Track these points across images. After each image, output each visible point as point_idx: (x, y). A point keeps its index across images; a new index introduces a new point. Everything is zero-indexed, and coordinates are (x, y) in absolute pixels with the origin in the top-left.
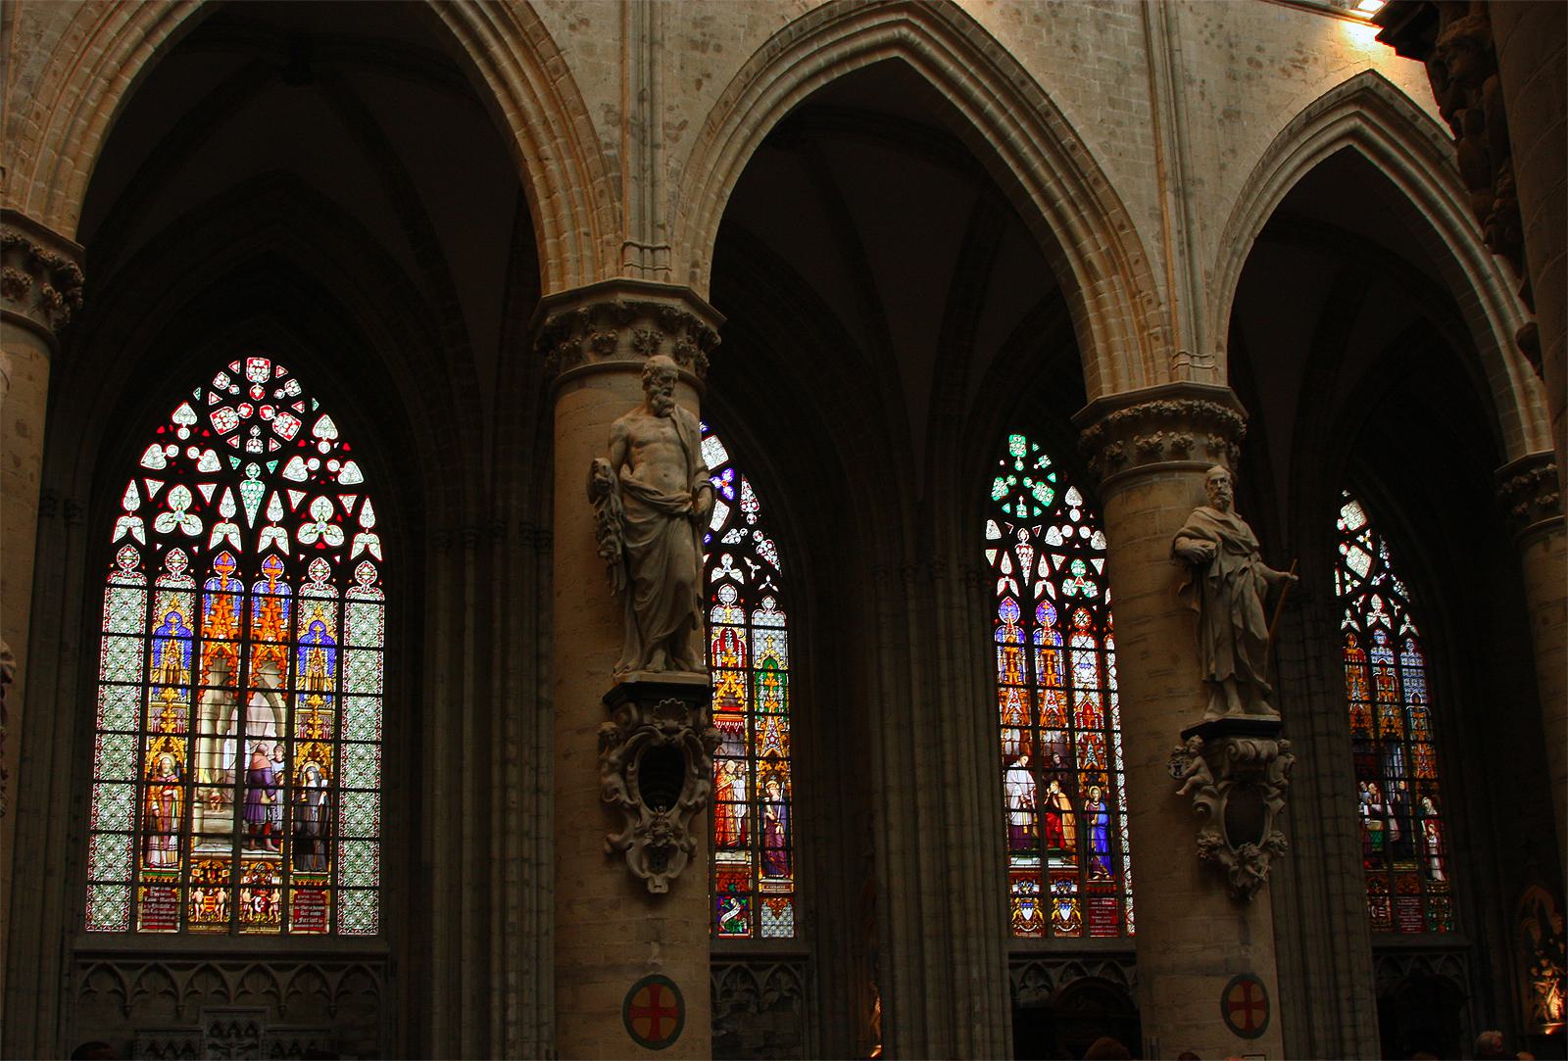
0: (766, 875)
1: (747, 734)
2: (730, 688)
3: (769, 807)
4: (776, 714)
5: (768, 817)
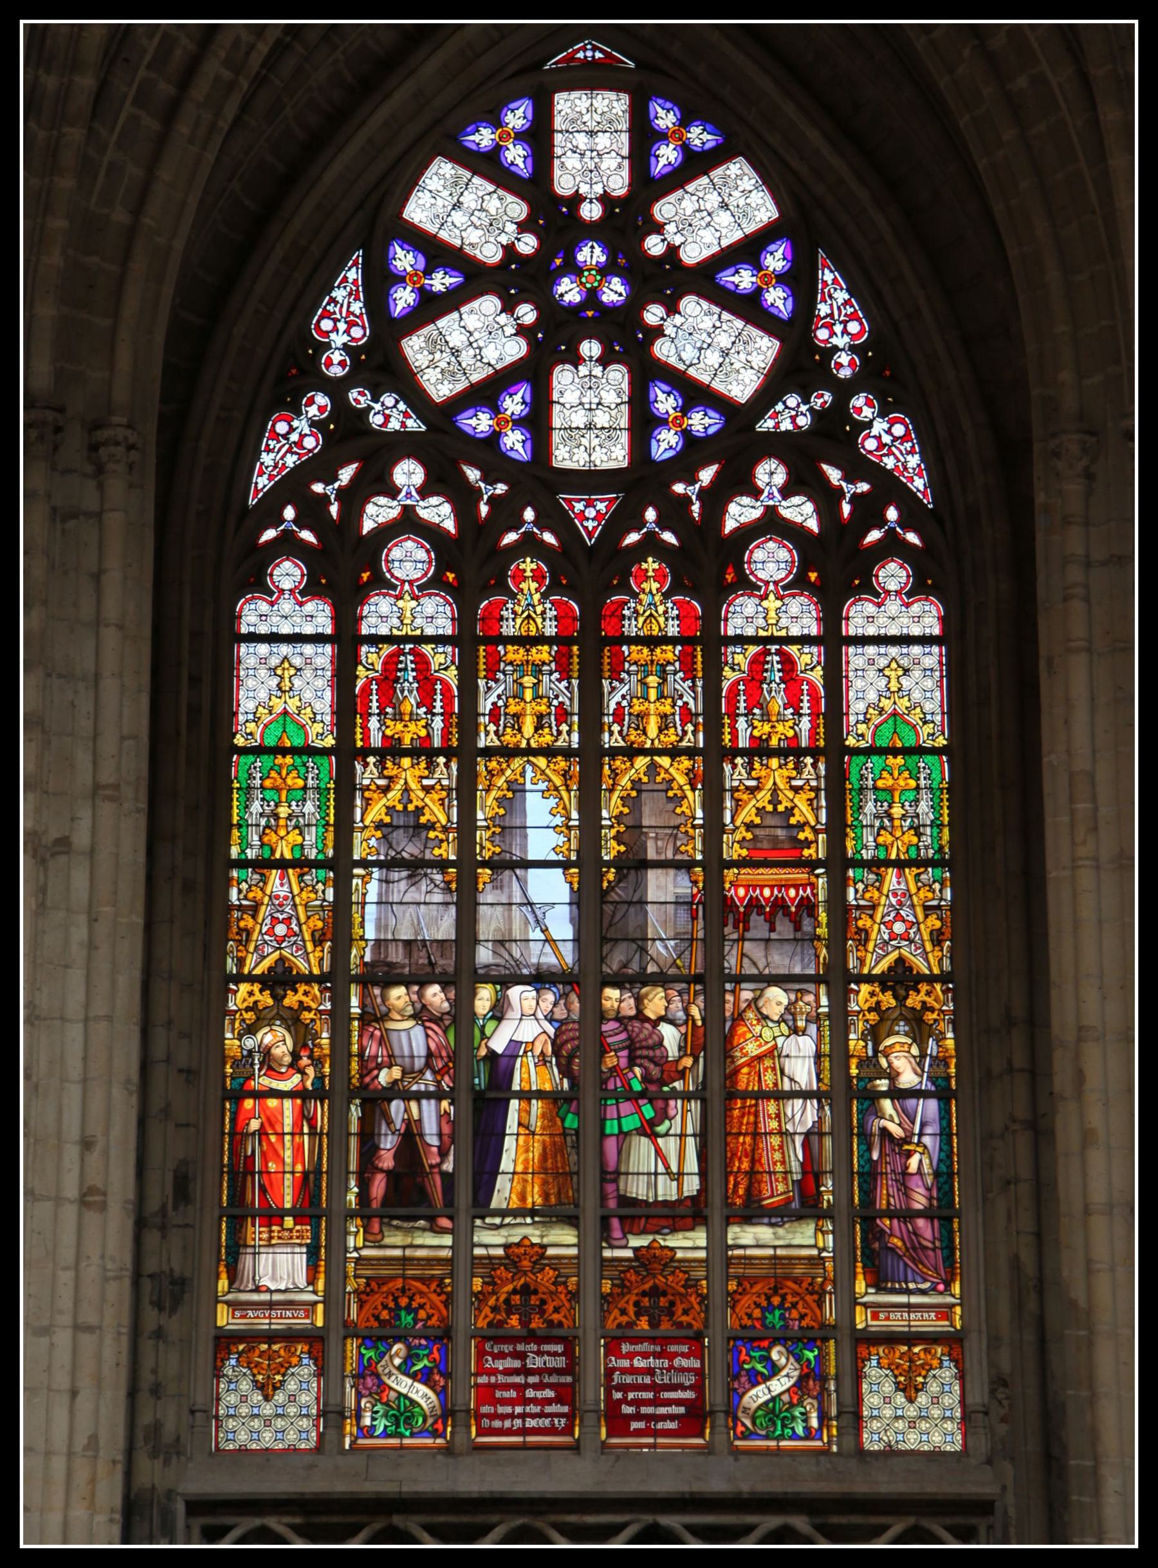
0: (878, 1283)
1: (823, 917)
2: (775, 801)
3: (887, 1105)
4: (910, 863)
5: (884, 1132)
